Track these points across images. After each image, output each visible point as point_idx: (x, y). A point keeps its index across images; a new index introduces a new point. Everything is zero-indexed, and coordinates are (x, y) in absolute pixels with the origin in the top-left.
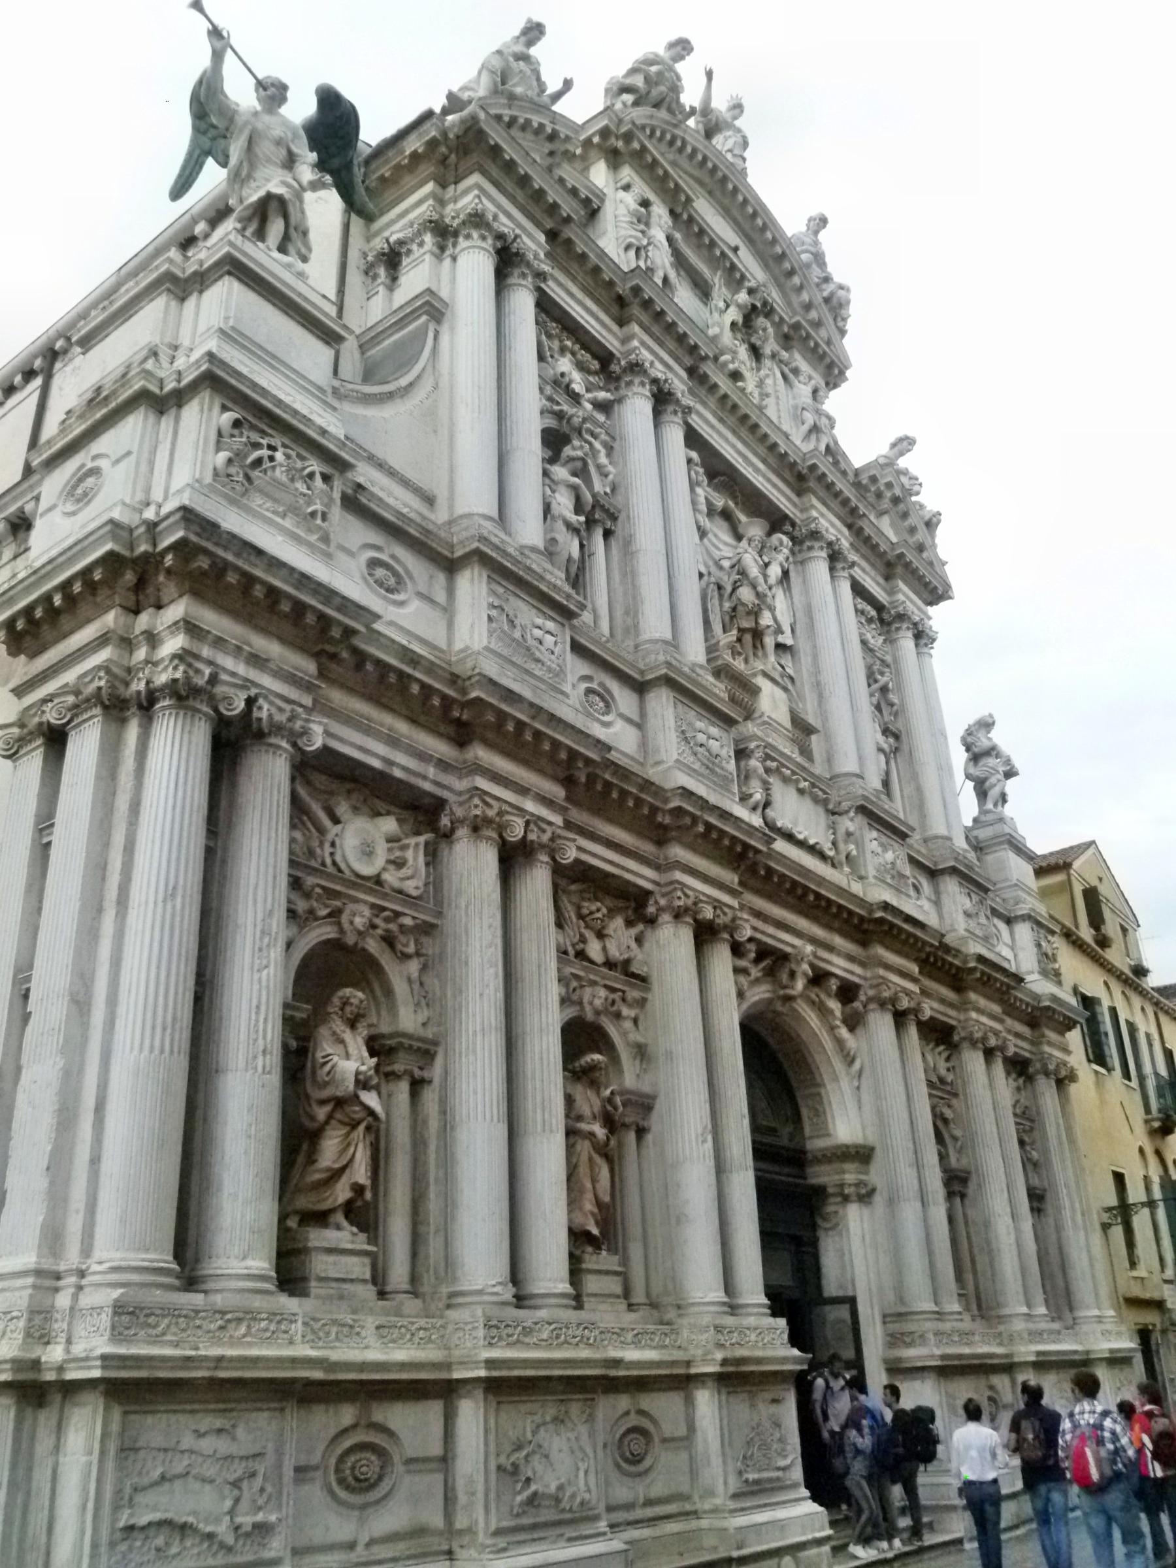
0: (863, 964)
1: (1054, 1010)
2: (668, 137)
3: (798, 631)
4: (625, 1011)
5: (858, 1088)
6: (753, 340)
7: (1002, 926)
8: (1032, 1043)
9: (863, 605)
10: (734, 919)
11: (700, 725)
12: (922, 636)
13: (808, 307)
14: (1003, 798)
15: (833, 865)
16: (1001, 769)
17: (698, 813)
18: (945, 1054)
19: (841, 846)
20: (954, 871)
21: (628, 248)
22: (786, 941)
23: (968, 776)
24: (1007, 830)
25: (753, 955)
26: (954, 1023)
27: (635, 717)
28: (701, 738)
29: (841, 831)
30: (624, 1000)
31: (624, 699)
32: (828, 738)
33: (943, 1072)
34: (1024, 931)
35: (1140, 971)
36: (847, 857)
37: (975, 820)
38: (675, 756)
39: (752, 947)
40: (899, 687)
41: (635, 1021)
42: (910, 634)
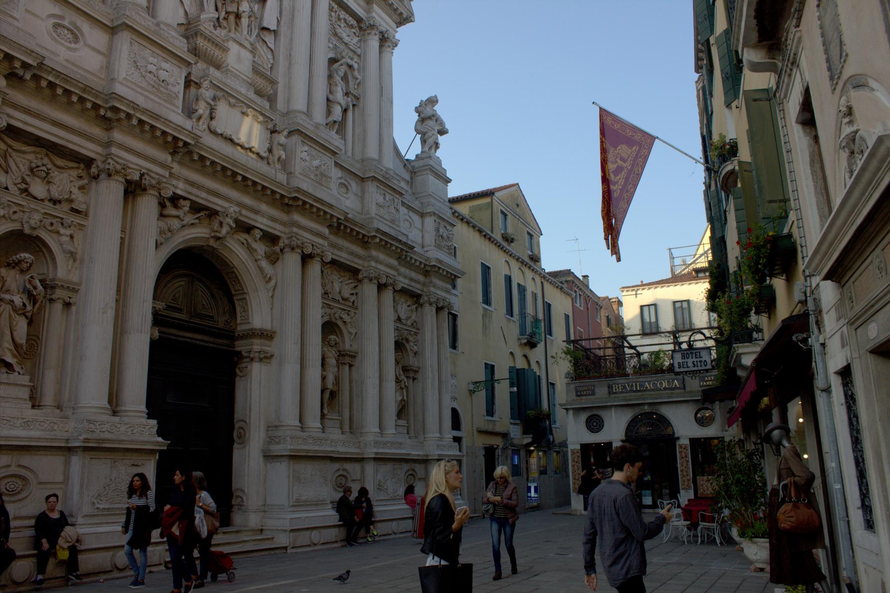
0: (283, 224)
1: (439, 268)
3: (282, 23)
4: (62, 231)
5: (272, 297)
7: (416, 219)
8: (424, 285)
9: (343, 14)
10: (159, 183)
11: (151, 59)
12: (386, 41)
14: (437, 145)
15: (268, 163)
16: (437, 128)
17: (132, 112)
18: (353, 285)
19: (275, 152)
20: (374, 178)
22: (218, 203)
23: (418, 131)
24: (431, 162)
25: (187, 209)
26: (360, 268)
27: (104, 50)
28: (151, 68)
29: (276, 142)
30: (62, 224)
31: (96, 37)
32: (289, 87)
33: (346, 294)
34: (430, 222)
35: (535, 259)
36: (279, 158)
37: (417, 156)
38: (124, 75)
39: (188, 203)
40: (363, 69)
41: (72, 237)
42: (377, 38)
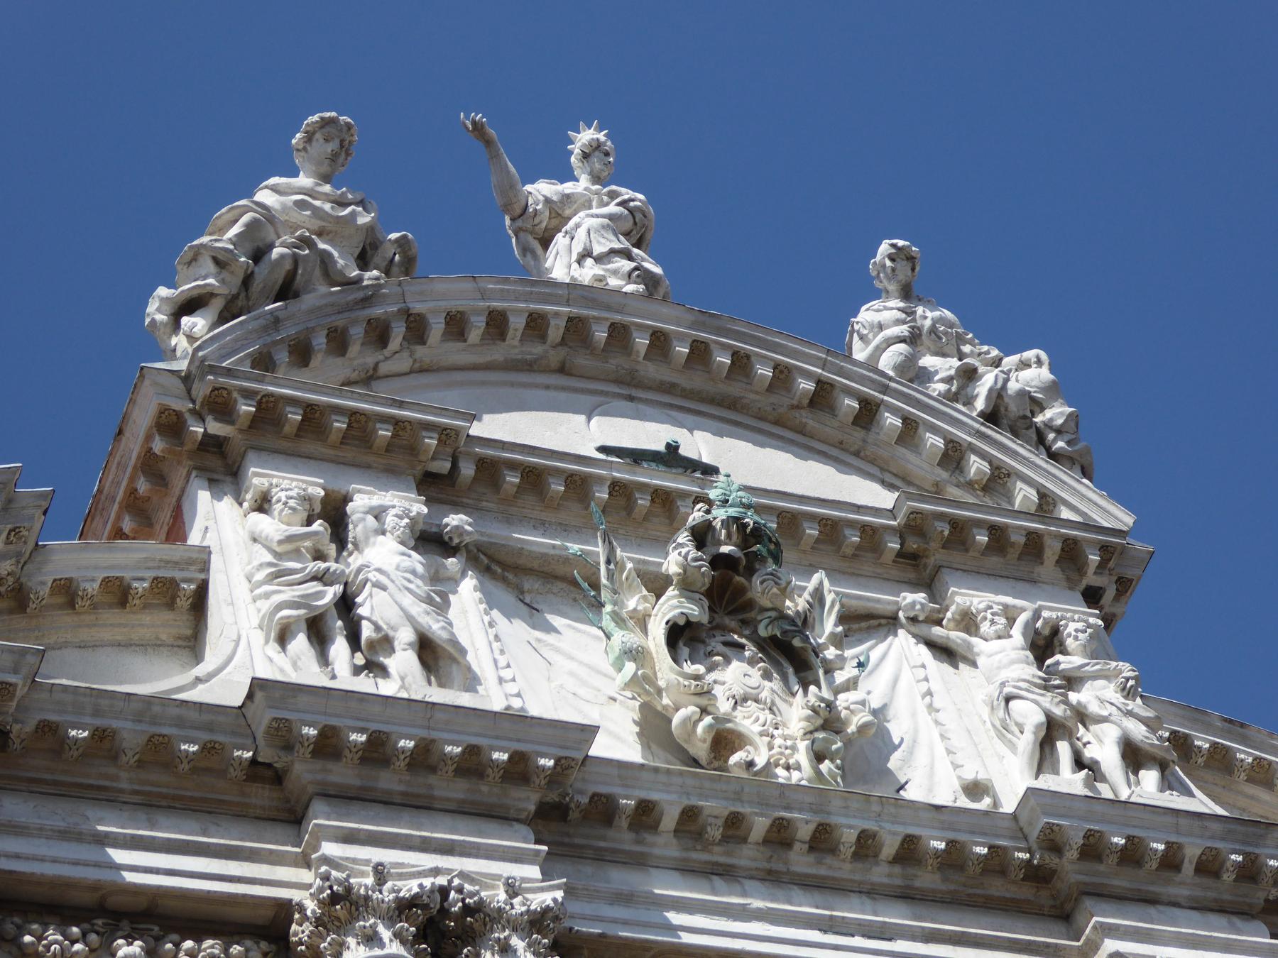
2: (357, 332)
6: (763, 632)
13: (953, 456)
21: (283, 639)
